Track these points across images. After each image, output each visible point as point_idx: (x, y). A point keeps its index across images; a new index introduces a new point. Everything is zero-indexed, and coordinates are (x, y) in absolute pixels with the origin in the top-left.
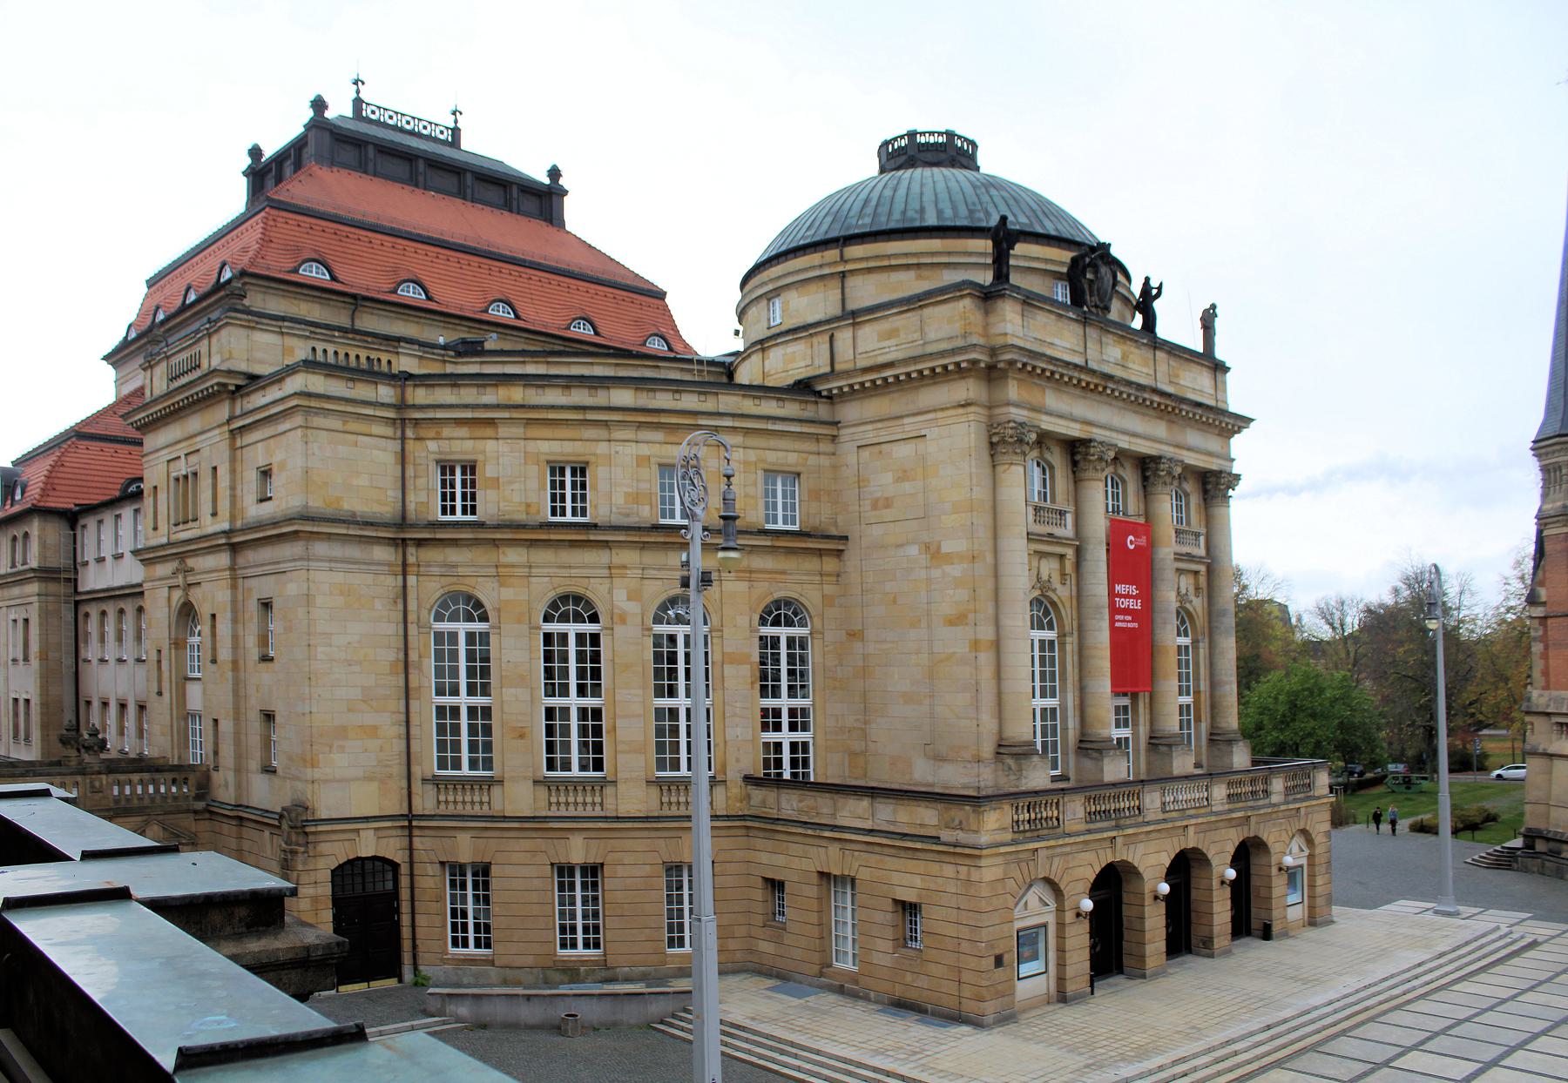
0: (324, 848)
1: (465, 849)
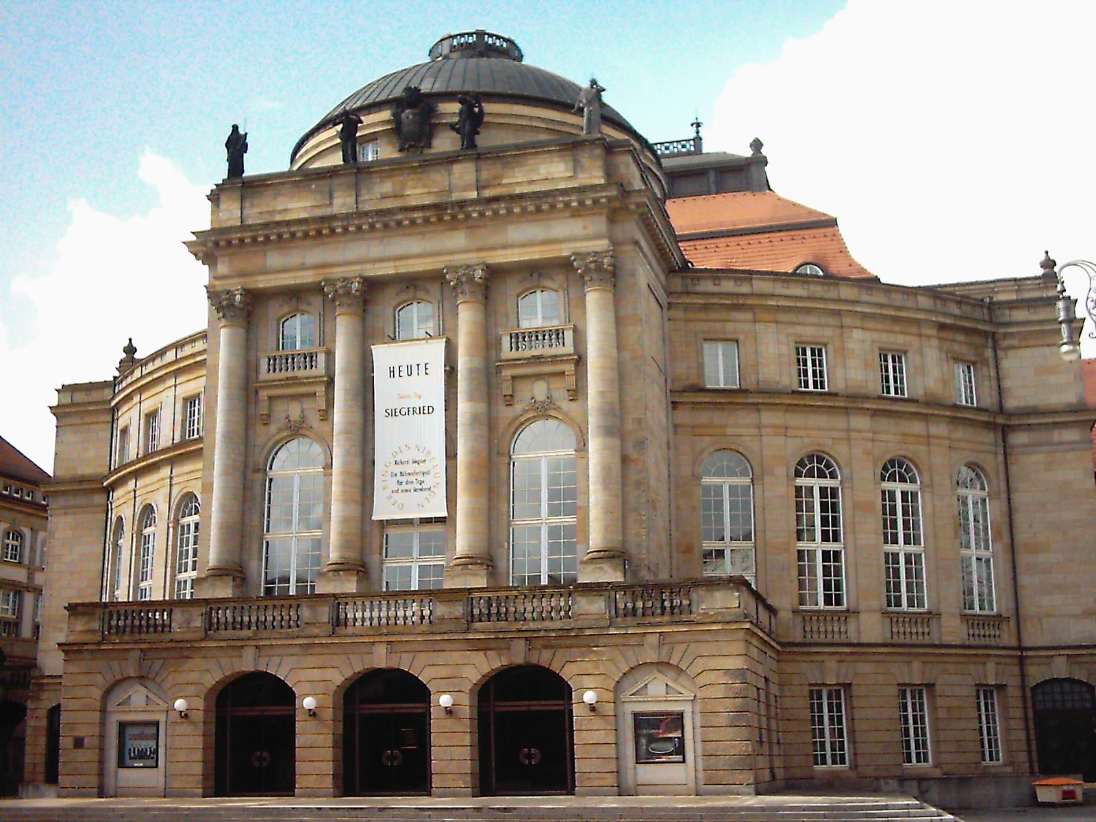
0: (44, 695)
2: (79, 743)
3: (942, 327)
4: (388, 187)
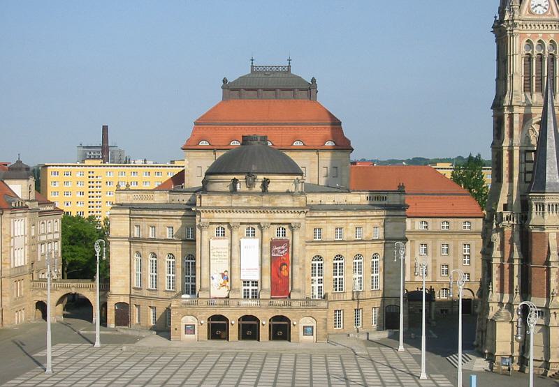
1: (138, 302)
2: (176, 329)
3: (372, 219)
4: (246, 200)
